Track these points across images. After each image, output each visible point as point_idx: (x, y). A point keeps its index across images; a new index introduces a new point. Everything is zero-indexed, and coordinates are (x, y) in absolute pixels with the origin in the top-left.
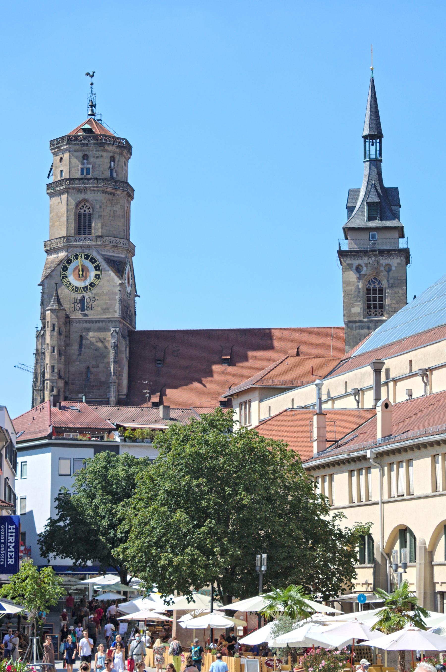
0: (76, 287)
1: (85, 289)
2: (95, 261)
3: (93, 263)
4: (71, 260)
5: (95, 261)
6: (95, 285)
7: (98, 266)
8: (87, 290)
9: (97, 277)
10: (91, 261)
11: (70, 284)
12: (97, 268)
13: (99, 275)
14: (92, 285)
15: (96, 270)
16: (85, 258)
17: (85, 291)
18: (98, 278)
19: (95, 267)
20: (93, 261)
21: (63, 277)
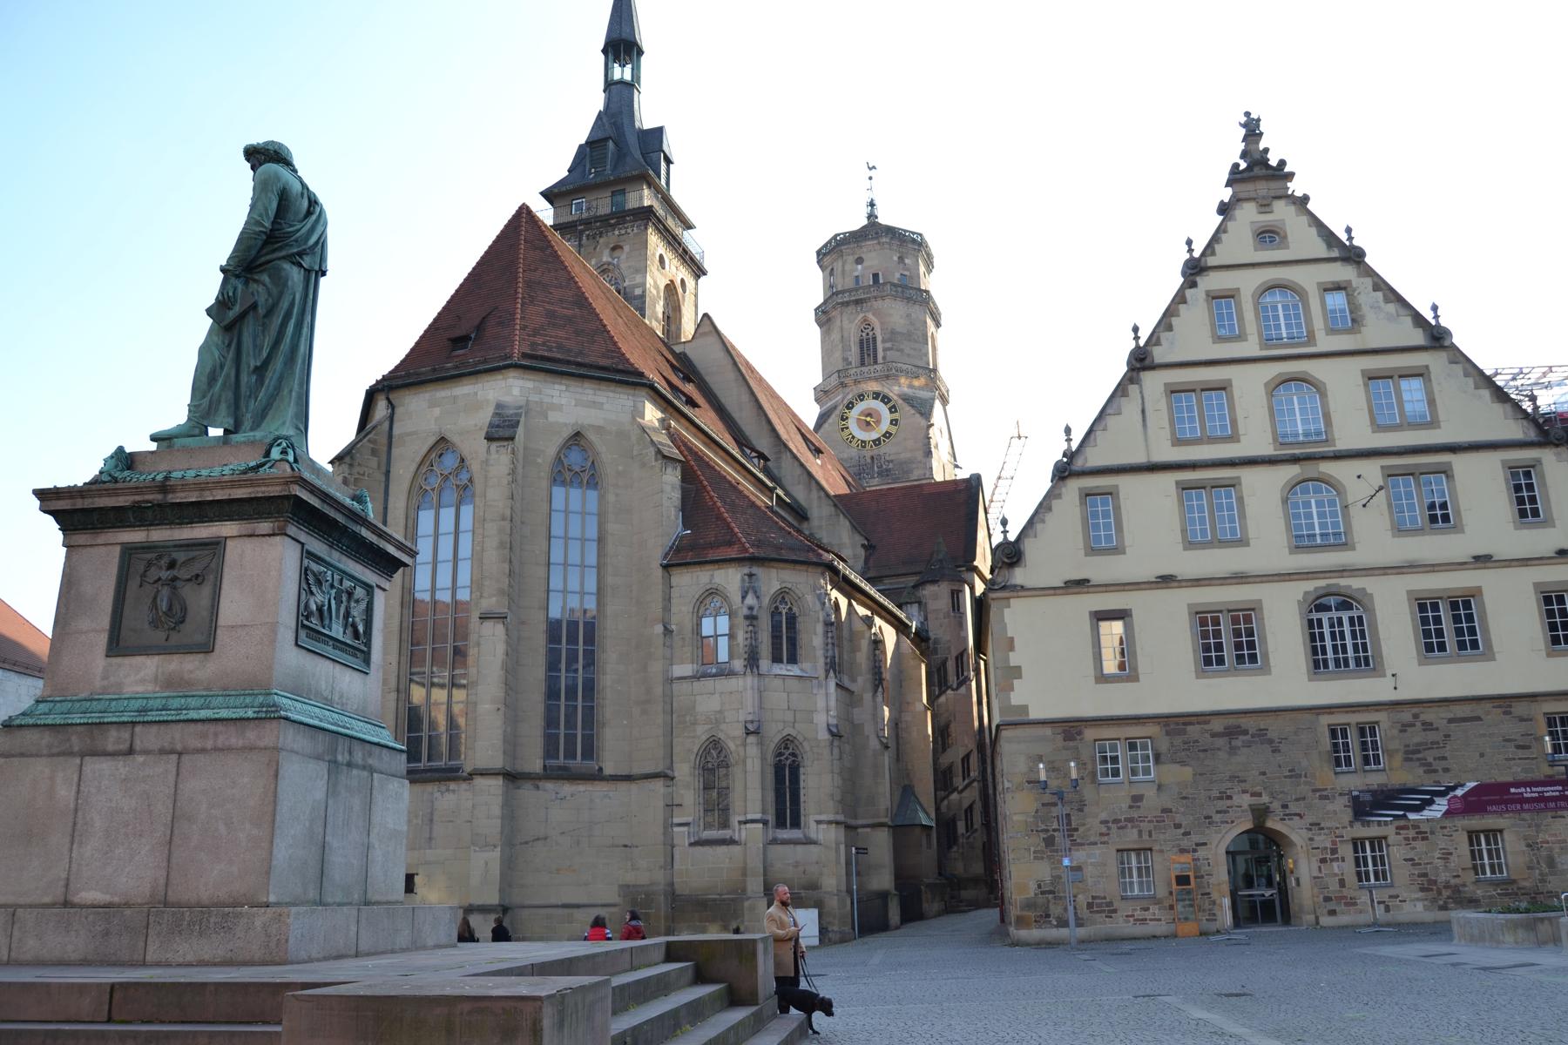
0: (862, 441)
1: (877, 442)
2: (890, 401)
3: (886, 404)
4: (852, 403)
5: (890, 401)
6: (891, 434)
7: (894, 406)
8: (880, 444)
9: (894, 422)
10: (882, 401)
11: (853, 437)
12: (893, 409)
13: (896, 420)
14: (887, 435)
15: (891, 412)
16: (874, 398)
17: (876, 445)
18: (896, 425)
19: (890, 409)
20: (886, 399)
21: (842, 430)
